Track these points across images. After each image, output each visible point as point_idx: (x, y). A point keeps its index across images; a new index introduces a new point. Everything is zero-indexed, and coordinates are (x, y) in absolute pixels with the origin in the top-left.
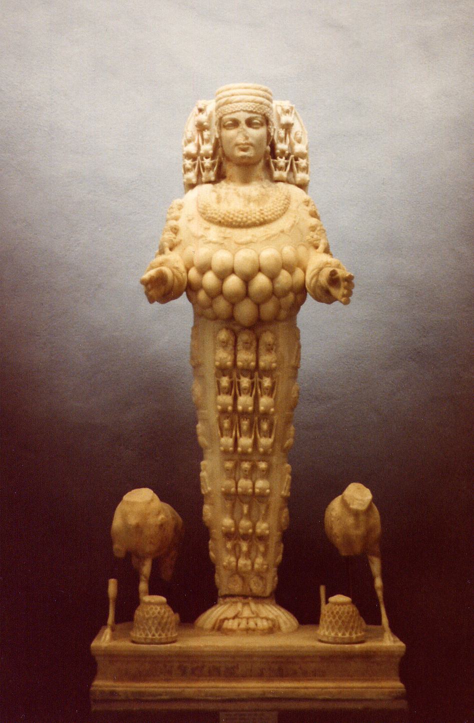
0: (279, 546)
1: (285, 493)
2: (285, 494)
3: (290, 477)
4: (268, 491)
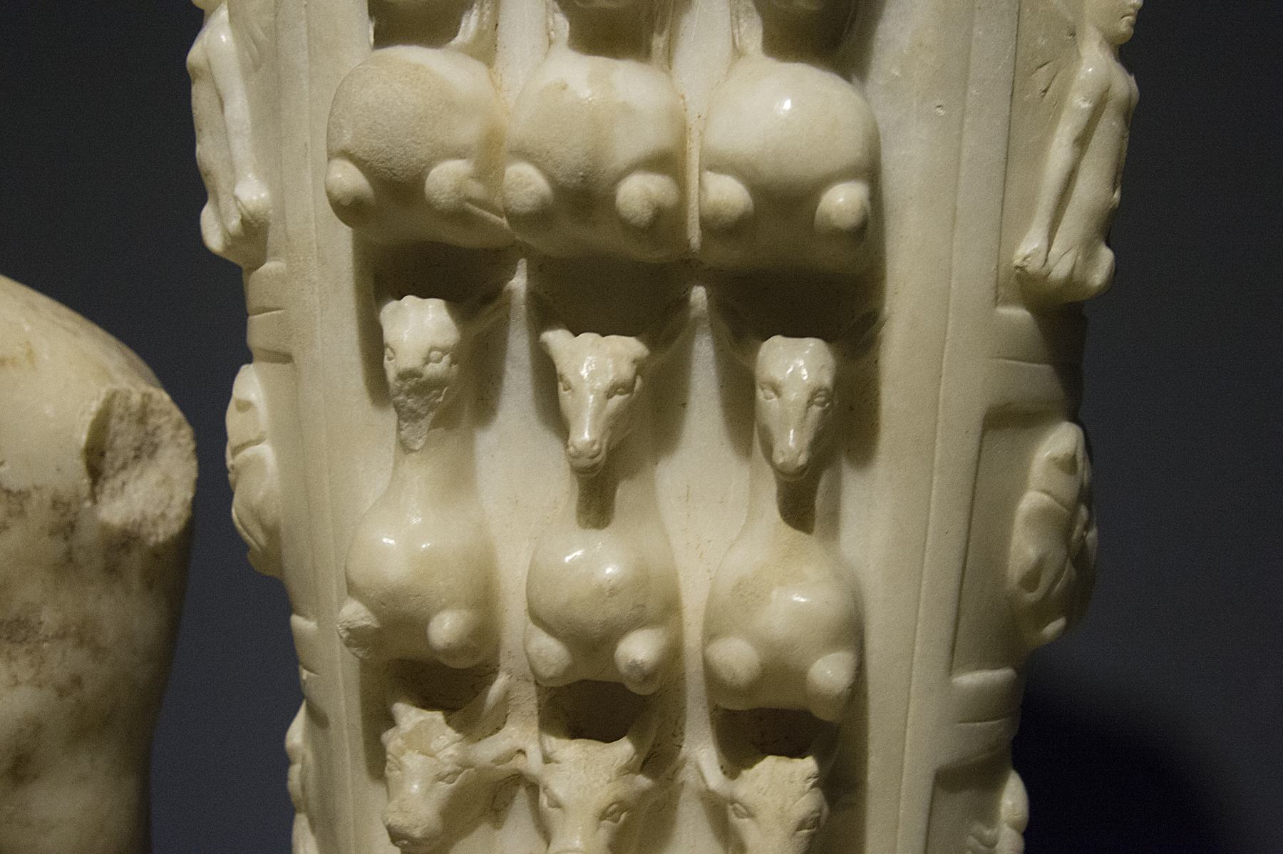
0: (987, 814)
1: (1060, 248)
2: (1061, 269)
3: (1123, 85)
4: (842, 201)
